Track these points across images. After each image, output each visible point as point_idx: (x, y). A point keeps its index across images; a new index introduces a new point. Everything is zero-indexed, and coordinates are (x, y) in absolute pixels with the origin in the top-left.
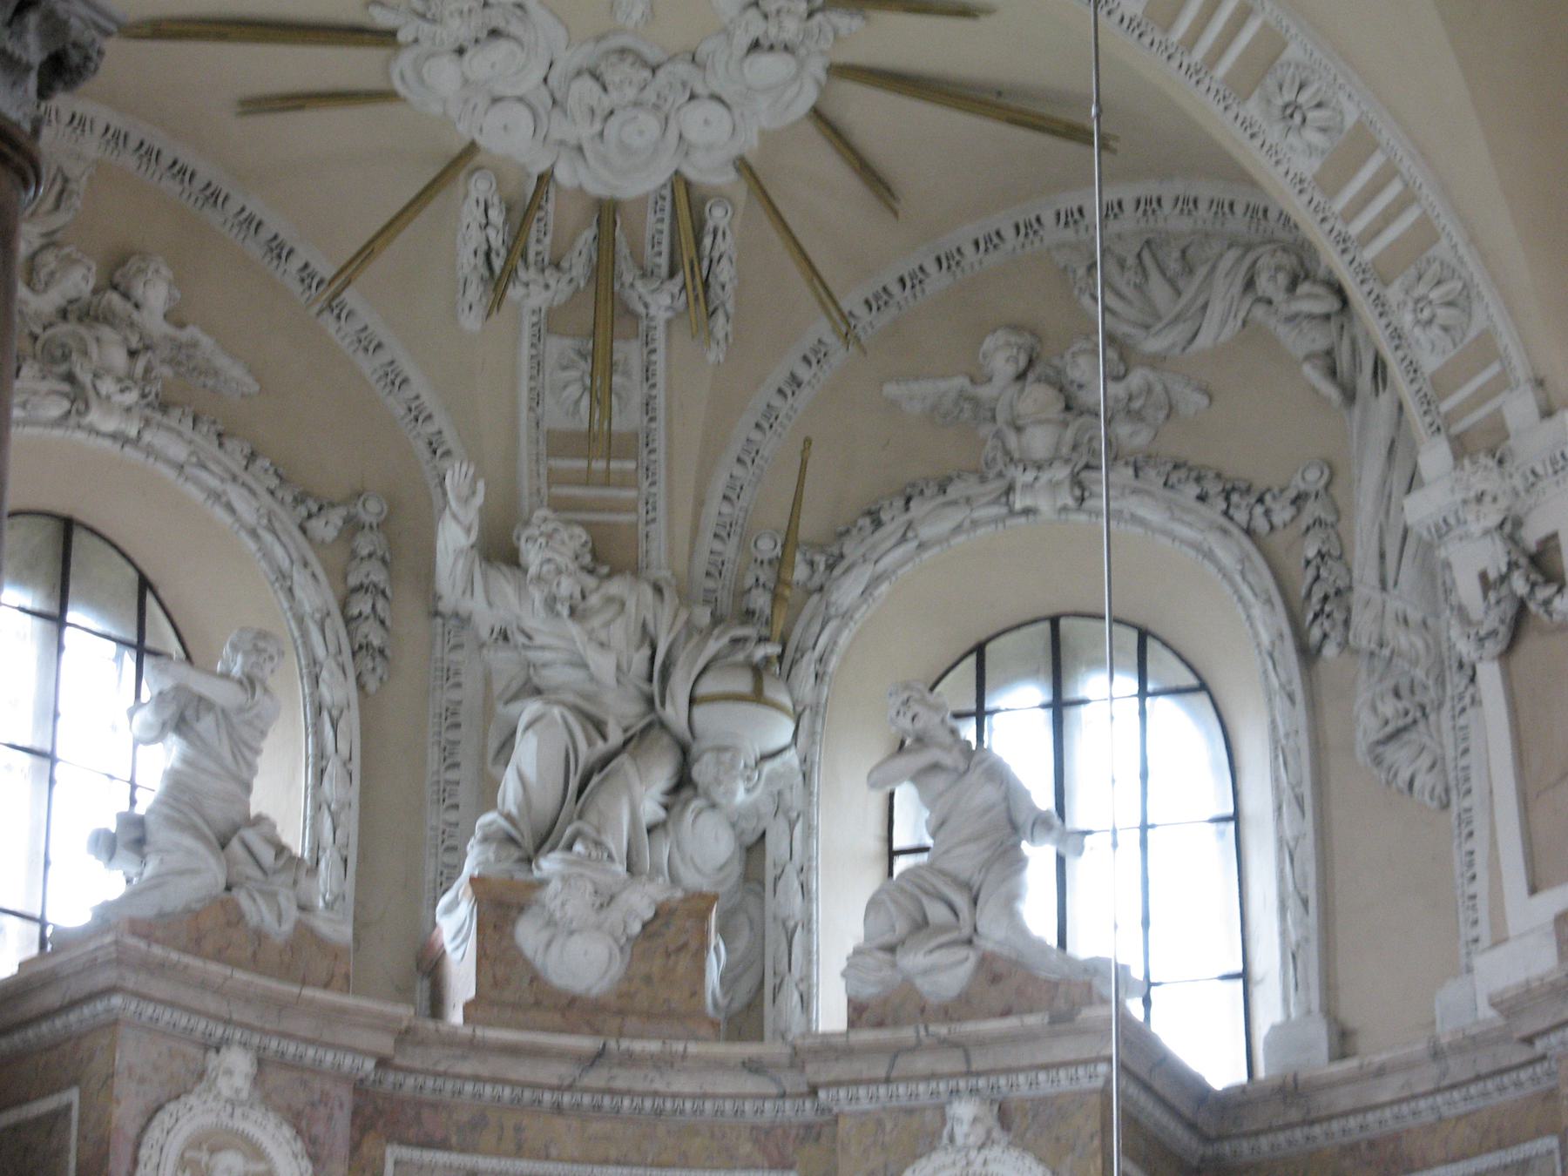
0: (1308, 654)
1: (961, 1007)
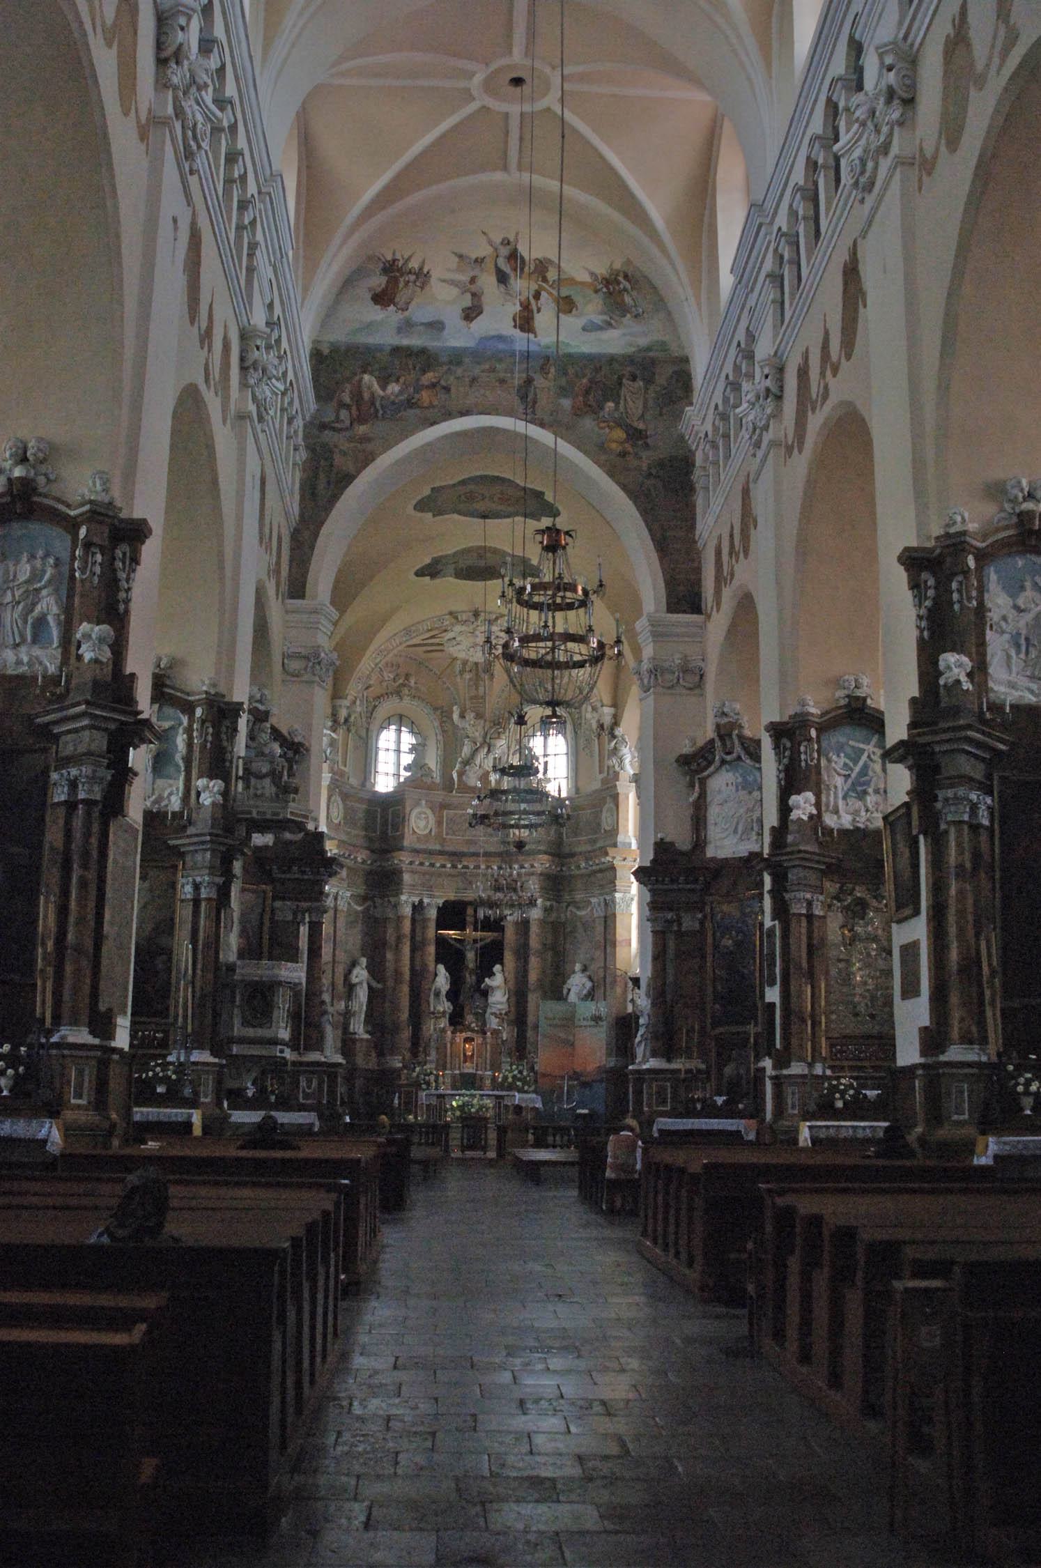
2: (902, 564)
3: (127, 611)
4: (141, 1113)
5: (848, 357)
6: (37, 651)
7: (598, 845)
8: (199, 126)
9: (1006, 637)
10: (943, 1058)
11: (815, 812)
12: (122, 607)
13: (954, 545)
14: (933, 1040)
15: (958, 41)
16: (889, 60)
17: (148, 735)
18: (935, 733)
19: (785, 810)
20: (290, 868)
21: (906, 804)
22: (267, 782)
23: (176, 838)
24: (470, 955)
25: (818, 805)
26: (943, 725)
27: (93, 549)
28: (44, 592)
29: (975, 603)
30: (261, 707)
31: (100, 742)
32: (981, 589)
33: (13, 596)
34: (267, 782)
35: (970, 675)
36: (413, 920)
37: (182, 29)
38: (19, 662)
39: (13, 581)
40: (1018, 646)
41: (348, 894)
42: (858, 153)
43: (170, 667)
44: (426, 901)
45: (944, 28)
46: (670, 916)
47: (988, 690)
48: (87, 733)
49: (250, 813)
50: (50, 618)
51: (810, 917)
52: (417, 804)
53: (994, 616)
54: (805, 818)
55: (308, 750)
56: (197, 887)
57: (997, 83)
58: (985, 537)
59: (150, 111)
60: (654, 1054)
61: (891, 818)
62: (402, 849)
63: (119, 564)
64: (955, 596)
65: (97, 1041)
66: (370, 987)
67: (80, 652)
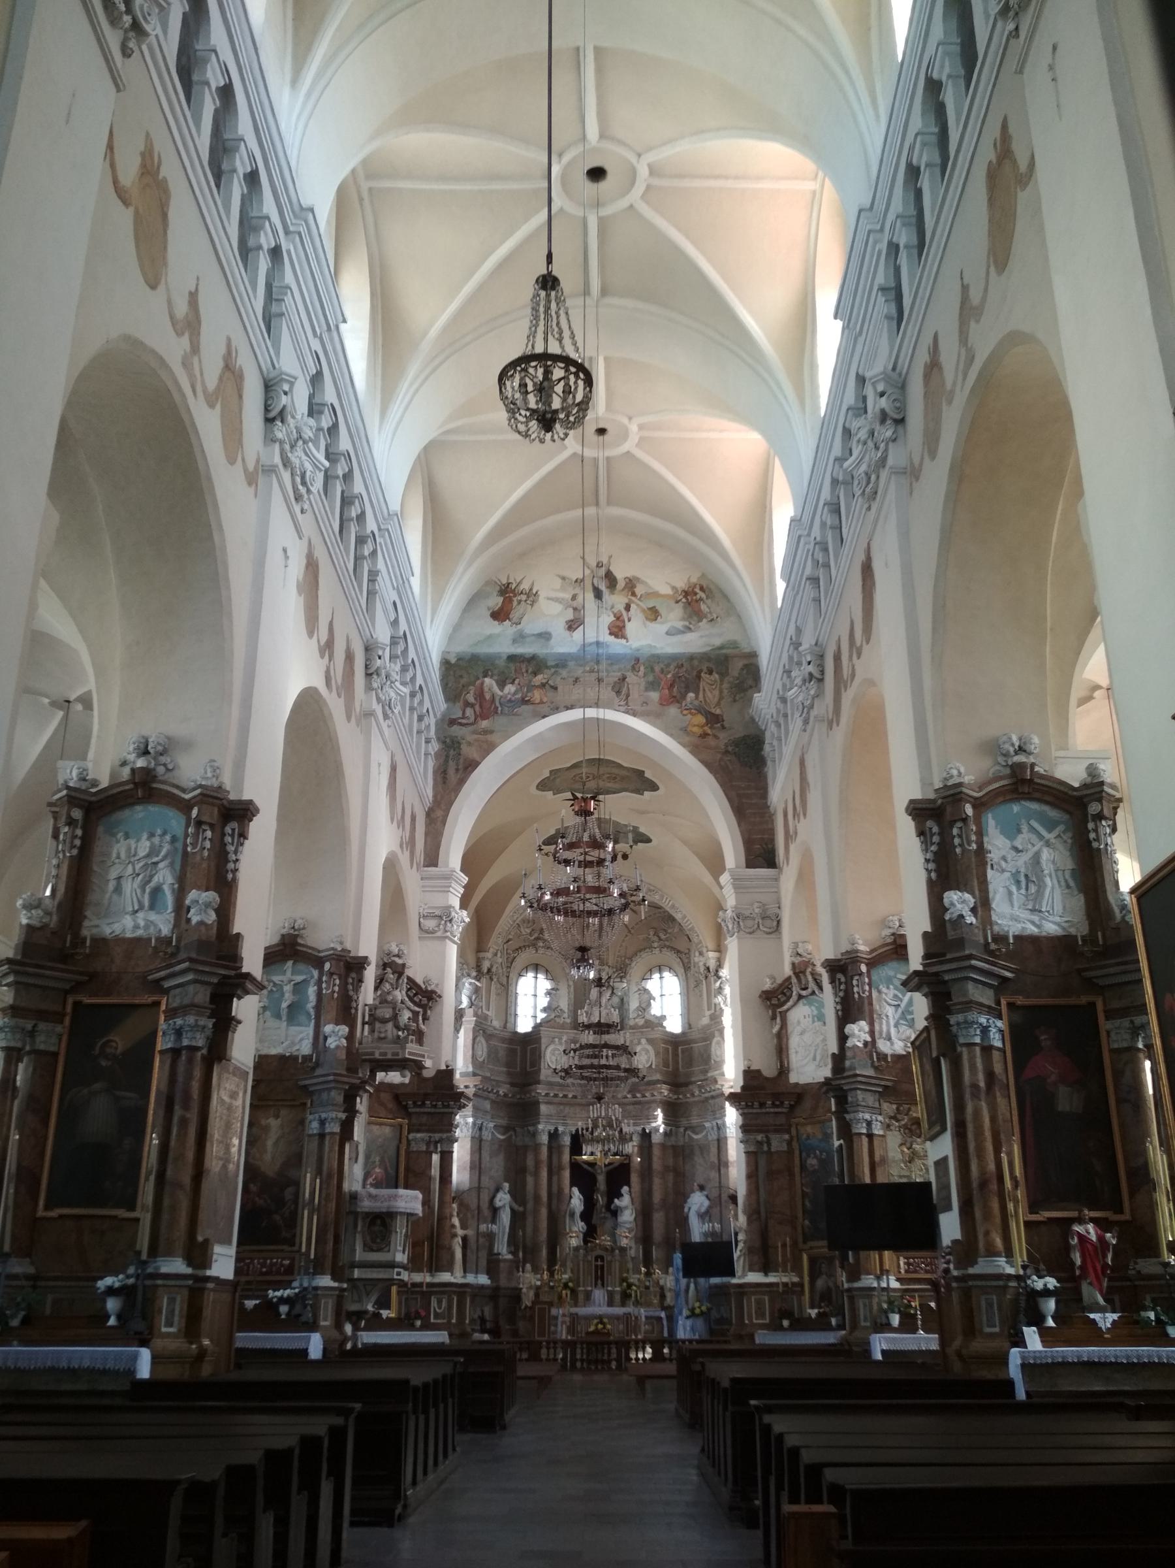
0: (686, 975)
1: (642, 1027)
2: (910, 815)
3: (234, 880)
4: (247, 1339)
5: (868, 642)
6: (153, 916)
7: (709, 1075)
8: (308, 474)
9: (1007, 875)
10: (971, 1271)
11: (869, 1039)
12: (230, 876)
13: (953, 795)
14: (967, 1250)
15: (933, 367)
16: (880, 388)
17: (249, 986)
18: (941, 963)
19: (843, 1038)
20: (423, 1105)
21: (926, 1029)
22: (390, 1025)
23: (305, 1079)
24: (601, 1179)
25: (872, 1033)
26: (949, 956)
27: (204, 827)
28: (161, 865)
29: (974, 846)
30: (399, 961)
31: (202, 995)
32: (980, 834)
33: (134, 869)
34: (390, 1025)
35: (974, 910)
36: (550, 1148)
37: (286, 393)
38: (136, 927)
39: (134, 856)
40: (1018, 882)
41: (491, 1125)
42: (864, 467)
43: (304, 928)
44: (561, 1129)
45: (923, 357)
46: (760, 1137)
47: (991, 923)
48: (191, 988)
49: (372, 1054)
50: (166, 888)
51: (870, 1136)
52: (553, 1042)
53: (994, 856)
54: (860, 1045)
55: (440, 997)
56: (322, 1123)
57: (961, 397)
58: (980, 789)
59: (258, 461)
60: (751, 1270)
61: (917, 1043)
62: (538, 1082)
63: (228, 839)
64: (957, 841)
65: (189, 1271)
66: (512, 1210)
67: (189, 916)
